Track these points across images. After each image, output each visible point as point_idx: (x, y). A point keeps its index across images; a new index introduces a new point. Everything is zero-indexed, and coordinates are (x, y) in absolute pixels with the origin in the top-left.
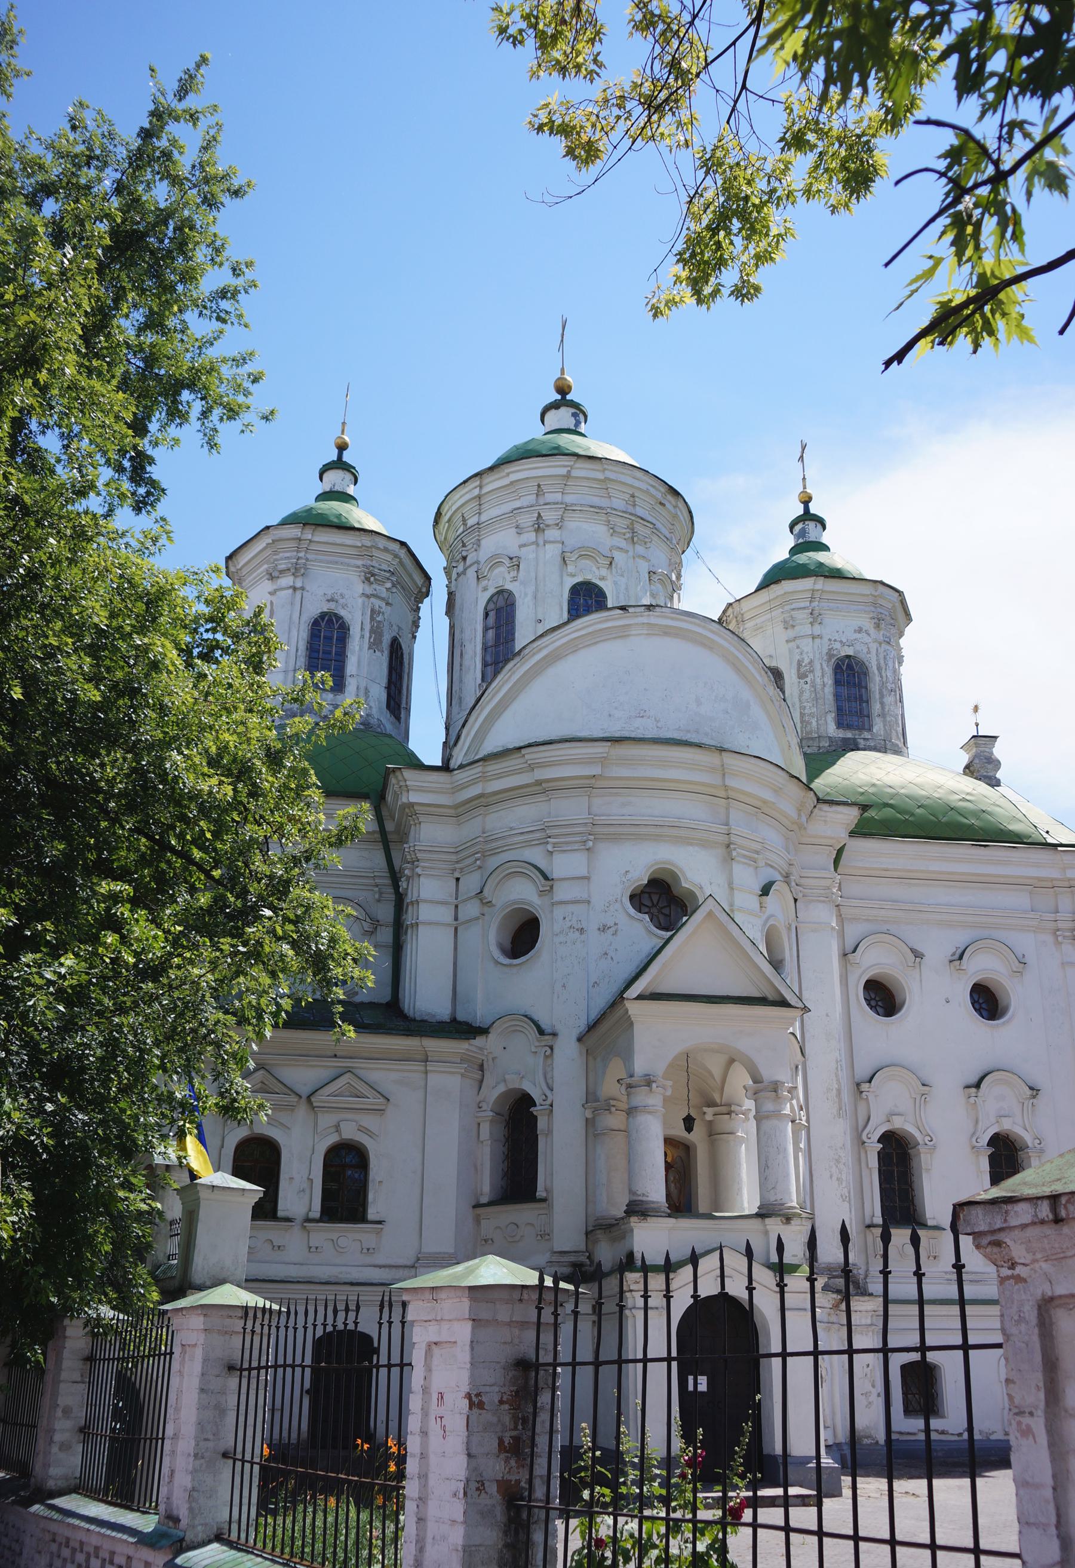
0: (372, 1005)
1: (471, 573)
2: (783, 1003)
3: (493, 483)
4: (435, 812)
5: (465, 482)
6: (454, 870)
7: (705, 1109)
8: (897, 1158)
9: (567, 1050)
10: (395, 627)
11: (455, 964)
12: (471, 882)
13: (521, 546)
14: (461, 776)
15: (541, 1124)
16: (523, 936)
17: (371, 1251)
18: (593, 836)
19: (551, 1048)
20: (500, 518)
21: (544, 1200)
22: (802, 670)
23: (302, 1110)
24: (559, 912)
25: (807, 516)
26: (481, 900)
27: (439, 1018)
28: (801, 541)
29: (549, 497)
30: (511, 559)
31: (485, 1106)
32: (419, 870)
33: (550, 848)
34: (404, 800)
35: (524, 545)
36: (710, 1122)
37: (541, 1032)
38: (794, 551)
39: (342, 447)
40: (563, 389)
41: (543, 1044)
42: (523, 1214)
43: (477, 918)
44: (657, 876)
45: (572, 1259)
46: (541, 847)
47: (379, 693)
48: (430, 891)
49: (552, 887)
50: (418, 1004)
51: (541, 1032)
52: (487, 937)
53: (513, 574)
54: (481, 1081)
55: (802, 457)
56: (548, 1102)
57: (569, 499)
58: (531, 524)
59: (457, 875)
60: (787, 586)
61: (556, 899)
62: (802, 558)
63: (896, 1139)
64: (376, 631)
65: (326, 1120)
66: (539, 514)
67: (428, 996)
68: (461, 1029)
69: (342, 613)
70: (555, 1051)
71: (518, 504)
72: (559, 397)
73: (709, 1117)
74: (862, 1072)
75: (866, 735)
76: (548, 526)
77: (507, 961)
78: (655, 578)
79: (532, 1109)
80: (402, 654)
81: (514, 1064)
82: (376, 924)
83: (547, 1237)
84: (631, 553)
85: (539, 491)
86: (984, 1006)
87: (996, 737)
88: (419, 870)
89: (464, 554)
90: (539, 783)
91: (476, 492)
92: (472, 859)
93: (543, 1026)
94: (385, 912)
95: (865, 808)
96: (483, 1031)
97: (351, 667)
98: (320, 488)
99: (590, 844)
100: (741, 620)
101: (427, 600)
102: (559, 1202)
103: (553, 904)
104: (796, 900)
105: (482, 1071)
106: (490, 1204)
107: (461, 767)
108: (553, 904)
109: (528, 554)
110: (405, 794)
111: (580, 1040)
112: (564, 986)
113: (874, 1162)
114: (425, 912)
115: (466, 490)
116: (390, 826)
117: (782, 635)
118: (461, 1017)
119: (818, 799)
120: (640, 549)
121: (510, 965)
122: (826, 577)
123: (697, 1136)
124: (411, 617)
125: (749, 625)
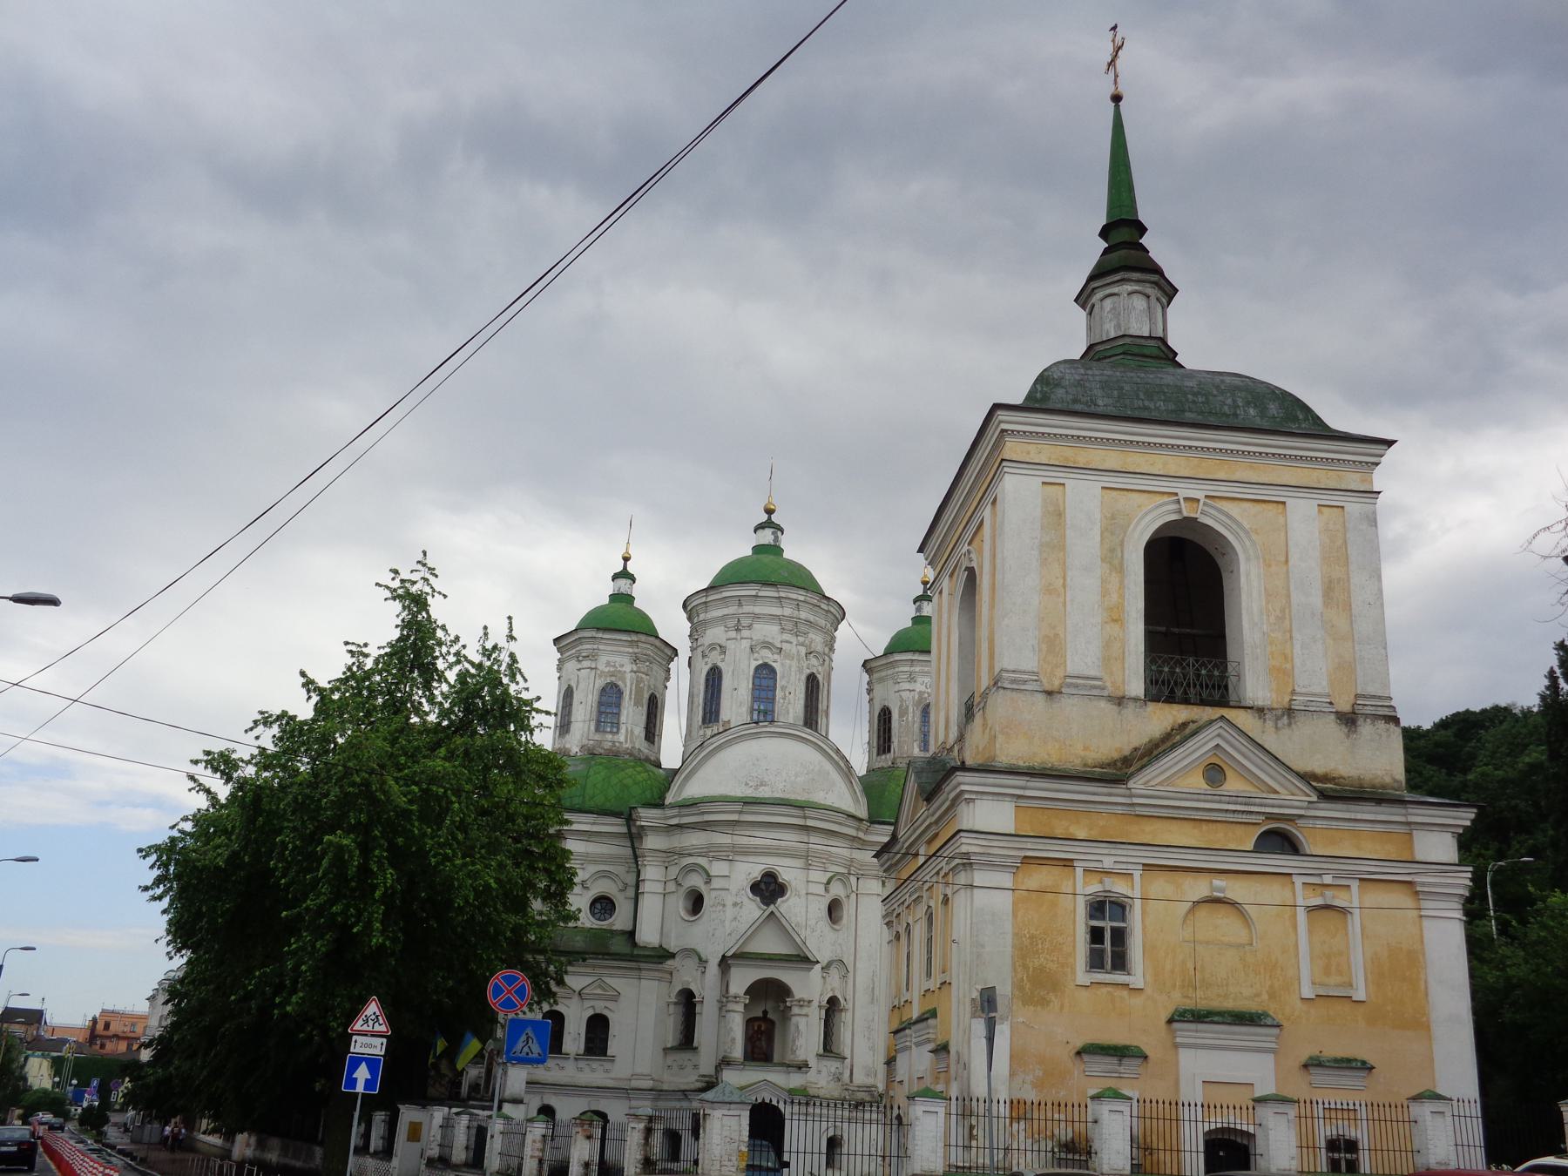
0: (623, 932)
9: (713, 968)
12: (674, 871)
14: (669, 812)
16: (696, 902)
18: (732, 854)
23: (576, 998)
24: (714, 894)
29: (747, 609)
39: (626, 559)
40: (769, 512)
42: (684, 1057)
47: (639, 731)
51: (700, 959)
57: (757, 610)
64: (639, 691)
65: (588, 1004)
69: (620, 683)
81: (686, 974)
94: (631, 879)
96: (673, 956)
97: (623, 719)
106: (672, 1049)
107: (672, 806)
109: (730, 645)
114: (646, 887)
116: (634, 830)
120: (801, 639)
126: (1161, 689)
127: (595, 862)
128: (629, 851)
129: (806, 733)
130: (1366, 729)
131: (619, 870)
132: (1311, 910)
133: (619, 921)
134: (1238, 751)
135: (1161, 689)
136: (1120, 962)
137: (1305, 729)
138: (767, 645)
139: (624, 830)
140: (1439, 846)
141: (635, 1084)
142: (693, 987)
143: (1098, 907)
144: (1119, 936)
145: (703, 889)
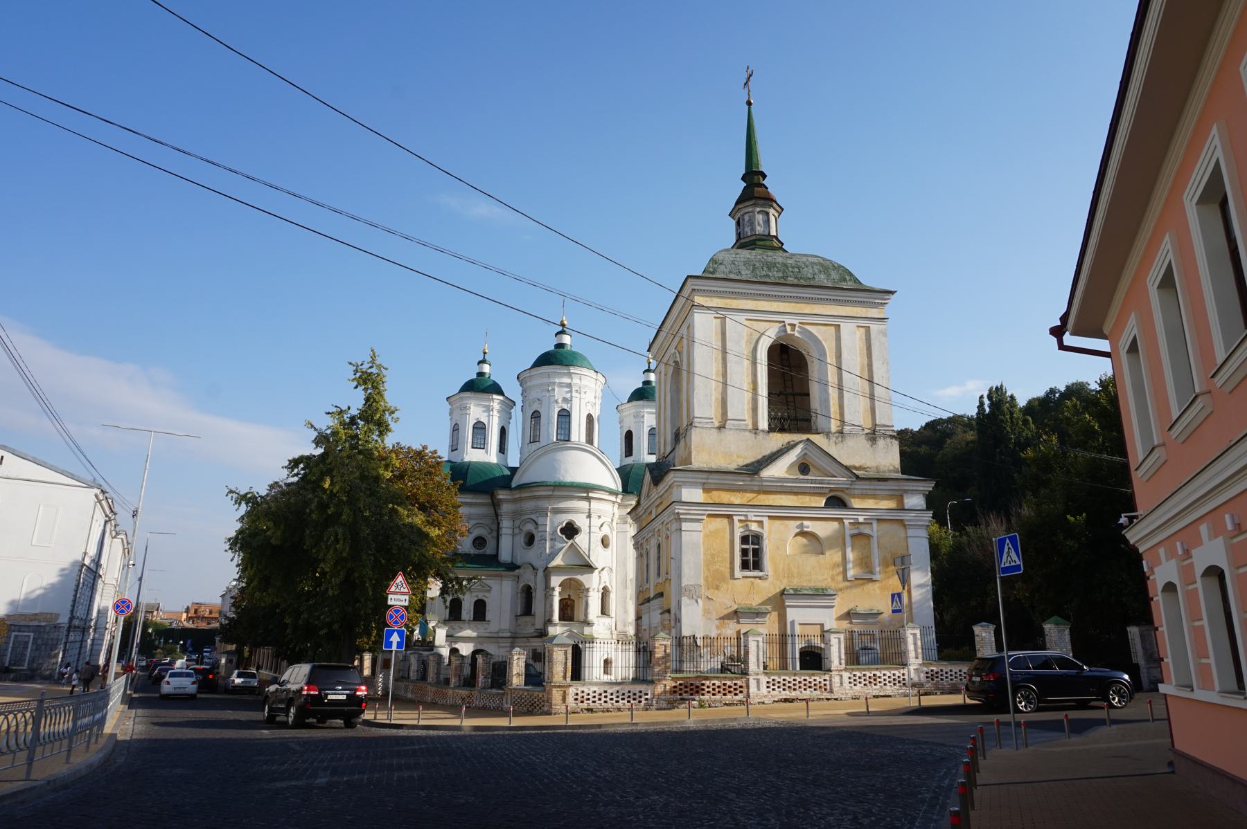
9: (540, 573)
12: (517, 523)
16: (530, 540)
42: (528, 618)
48: (506, 524)
52: (521, 540)
67: (505, 556)
81: (527, 577)
96: (519, 567)
102: (537, 615)
114: (504, 531)
126: (779, 424)
128: (490, 511)
129: (588, 447)
130: (881, 442)
132: (853, 536)
133: (489, 550)
134: (815, 458)
135: (779, 424)
136: (757, 565)
137: (850, 442)
138: (565, 400)
139: (490, 501)
140: (916, 501)
143: (745, 539)
144: (757, 553)
145: (535, 532)
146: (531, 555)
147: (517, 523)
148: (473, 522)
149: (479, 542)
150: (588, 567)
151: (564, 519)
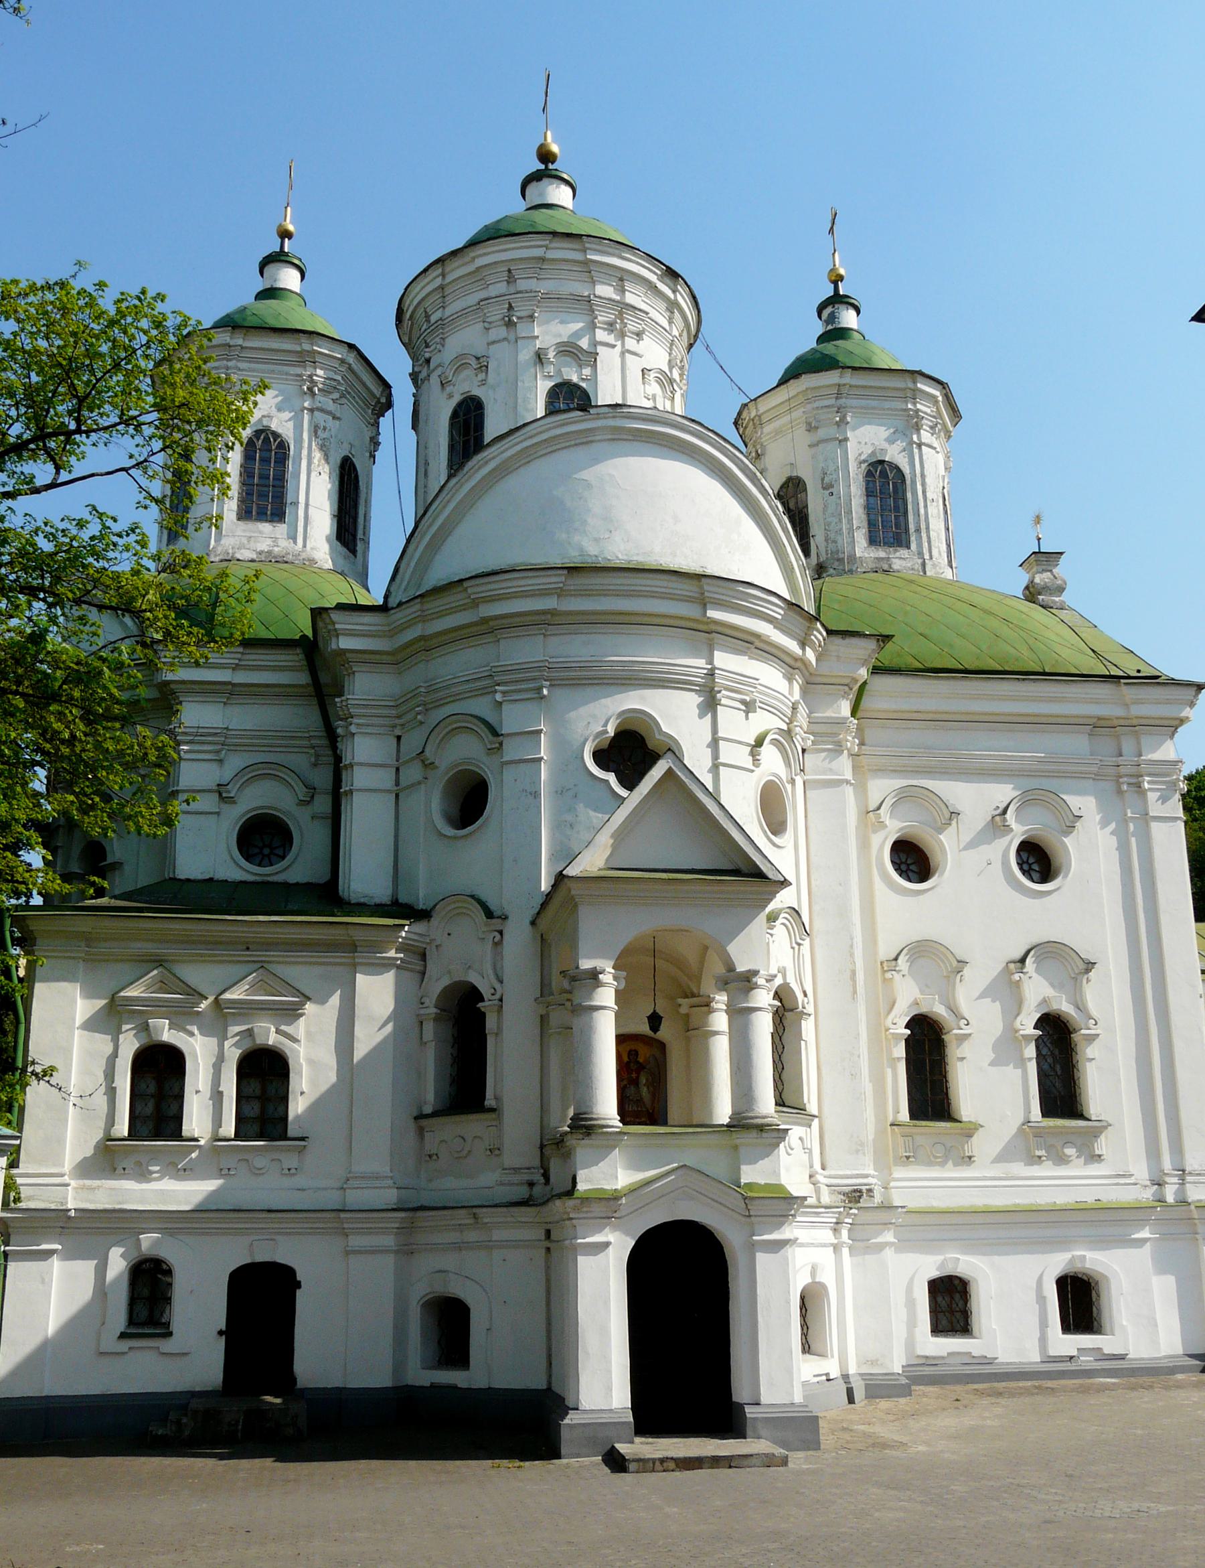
1: (435, 380)
2: (759, 875)
3: (457, 270)
4: (369, 658)
5: (425, 270)
6: (394, 726)
7: (680, 1001)
8: (927, 1046)
9: (518, 935)
10: (346, 446)
11: (396, 836)
12: (413, 741)
13: (488, 344)
14: (399, 616)
15: (491, 1023)
16: (470, 801)
17: (293, 1171)
19: (501, 933)
20: (464, 313)
21: (492, 1110)
22: (826, 480)
24: (509, 774)
25: (838, 299)
26: (423, 761)
27: (378, 901)
28: (830, 327)
29: (522, 285)
30: (478, 359)
31: (427, 1001)
32: (353, 729)
33: (499, 697)
34: (334, 646)
35: (494, 342)
36: (687, 1015)
37: (489, 914)
38: (822, 339)
41: (493, 928)
42: (471, 1126)
43: (419, 783)
44: (622, 728)
45: (526, 1177)
46: (490, 697)
49: (501, 744)
50: (352, 887)
51: (489, 914)
52: (430, 804)
53: (482, 376)
54: (424, 973)
55: (832, 228)
56: (498, 996)
58: (501, 316)
59: (398, 732)
60: (808, 381)
61: (505, 759)
62: (829, 348)
63: (929, 1023)
66: (510, 304)
67: (365, 876)
68: (401, 909)
70: (506, 937)
71: (483, 294)
72: (543, 167)
73: (683, 1010)
74: (885, 951)
75: (903, 552)
76: (519, 318)
77: (451, 832)
78: (653, 374)
79: (480, 1005)
80: (357, 477)
81: (461, 953)
82: (312, 790)
83: (497, 1152)
84: (618, 349)
85: (511, 278)
86: (1035, 867)
87: (1061, 553)
88: (353, 729)
89: (427, 355)
90: (485, 620)
91: (439, 281)
92: (413, 714)
93: (492, 908)
94: (322, 778)
95: (886, 638)
98: (260, 285)
99: (545, 692)
100: (758, 422)
101: (389, 414)
103: (503, 764)
104: (804, 751)
105: (425, 961)
106: (435, 1114)
107: (400, 604)
108: (503, 764)
110: (334, 640)
111: (533, 923)
112: (515, 860)
113: (900, 1051)
114: (359, 778)
115: (427, 280)
116: (324, 678)
117: (802, 437)
118: (403, 899)
119: (830, 632)
120: (630, 343)
121: (455, 838)
122: (854, 368)
123: (664, 1033)
124: (368, 433)
125: (768, 429)
127: (235, 748)
131: (300, 761)
133: (300, 866)
139: (303, 678)
141: (355, 1197)
142: (474, 978)
146: (471, 862)
147: (413, 741)
148: (236, 762)
149: (262, 836)
150: (747, 878)
151: (600, 716)
